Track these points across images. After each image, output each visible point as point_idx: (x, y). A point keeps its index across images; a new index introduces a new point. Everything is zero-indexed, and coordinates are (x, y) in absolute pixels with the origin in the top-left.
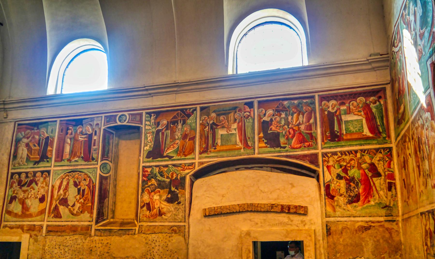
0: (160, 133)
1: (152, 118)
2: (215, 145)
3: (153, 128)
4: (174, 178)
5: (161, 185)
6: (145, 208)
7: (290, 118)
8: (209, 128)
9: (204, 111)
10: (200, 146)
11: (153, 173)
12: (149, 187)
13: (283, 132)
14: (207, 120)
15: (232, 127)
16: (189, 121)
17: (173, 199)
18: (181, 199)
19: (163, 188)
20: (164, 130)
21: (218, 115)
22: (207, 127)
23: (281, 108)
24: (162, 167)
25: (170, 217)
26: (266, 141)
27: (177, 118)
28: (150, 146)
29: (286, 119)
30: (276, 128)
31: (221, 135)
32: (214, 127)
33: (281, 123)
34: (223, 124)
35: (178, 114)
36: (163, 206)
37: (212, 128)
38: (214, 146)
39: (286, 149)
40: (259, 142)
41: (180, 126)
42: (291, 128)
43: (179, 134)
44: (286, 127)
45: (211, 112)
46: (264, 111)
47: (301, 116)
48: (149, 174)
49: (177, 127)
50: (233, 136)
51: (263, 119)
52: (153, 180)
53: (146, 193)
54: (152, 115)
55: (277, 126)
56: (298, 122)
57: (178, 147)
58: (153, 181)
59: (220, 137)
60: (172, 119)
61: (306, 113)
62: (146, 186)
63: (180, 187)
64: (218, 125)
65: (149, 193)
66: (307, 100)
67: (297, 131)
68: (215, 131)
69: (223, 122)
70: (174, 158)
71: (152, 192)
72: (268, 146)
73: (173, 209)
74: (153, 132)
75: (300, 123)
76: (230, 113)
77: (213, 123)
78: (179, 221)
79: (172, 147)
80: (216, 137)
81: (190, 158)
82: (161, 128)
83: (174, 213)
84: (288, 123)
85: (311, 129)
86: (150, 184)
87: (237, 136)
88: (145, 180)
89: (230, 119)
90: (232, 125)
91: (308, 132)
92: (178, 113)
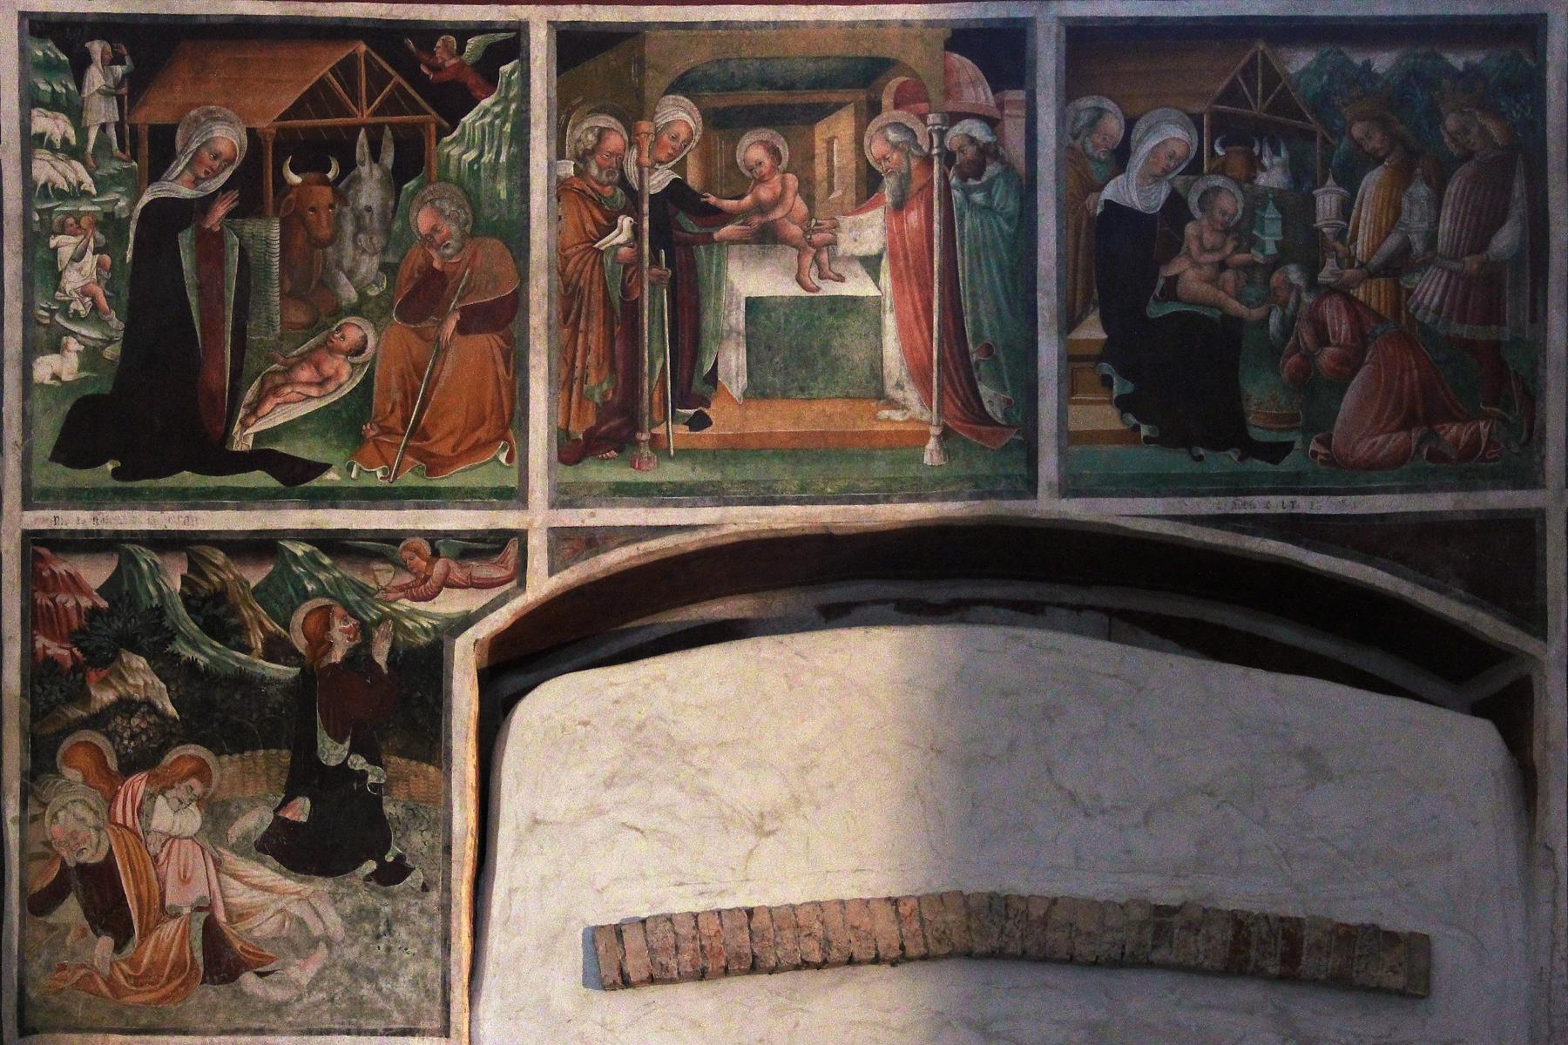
0: (185, 239)
1: (96, 78)
2: (698, 386)
4: (337, 656)
5: (219, 715)
6: (71, 911)
7: (1327, 201)
8: (636, 230)
9: (596, 67)
10: (568, 384)
11: (132, 598)
12: (98, 721)
13: (1265, 322)
14: (620, 157)
15: (847, 245)
16: (457, 152)
17: (339, 836)
20: (220, 210)
21: (725, 123)
22: (625, 222)
23: (1258, 109)
24: (219, 558)
25: (314, 984)
26: (1129, 387)
27: (343, 111)
28: (90, 357)
29: (1297, 207)
30: (1212, 281)
31: (753, 304)
32: (684, 226)
33: (1253, 242)
34: (761, 208)
35: (346, 70)
36: (240, 895)
37: (663, 234)
38: (684, 396)
39: (1288, 464)
40: (1071, 387)
41: (370, 192)
42: (1331, 290)
43: (368, 266)
44: (1294, 274)
45: (655, 82)
46: (1114, 125)
47: (1420, 190)
48: (95, 611)
49: (341, 197)
50: (855, 325)
51: (1108, 193)
52: (140, 662)
53: (73, 775)
54: (97, 48)
55: (1223, 265)
56: (1392, 242)
57: (368, 381)
58: (140, 676)
59: (738, 318)
60: (296, 110)
61: (1466, 169)
64: (725, 217)
65: (108, 782)
66: (1477, 57)
67: (1380, 319)
68: (692, 266)
69: (765, 193)
71: (129, 767)
72: (1144, 431)
73: (334, 922)
74: (110, 224)
75: (1405, 248)
76: (823, 111)
77: (677, 190)
78: (399, 1021)
79: (305, 374)
80: (708, 321)
82: (185, 192)
83: (351, 953)
84: (1306, 246)
85: (1492, 314)
86: (105, 696)
87: (890, 321)
88: (52, 663)
89: (820, 170)
90: (846, 222)
91: (1464, 331)
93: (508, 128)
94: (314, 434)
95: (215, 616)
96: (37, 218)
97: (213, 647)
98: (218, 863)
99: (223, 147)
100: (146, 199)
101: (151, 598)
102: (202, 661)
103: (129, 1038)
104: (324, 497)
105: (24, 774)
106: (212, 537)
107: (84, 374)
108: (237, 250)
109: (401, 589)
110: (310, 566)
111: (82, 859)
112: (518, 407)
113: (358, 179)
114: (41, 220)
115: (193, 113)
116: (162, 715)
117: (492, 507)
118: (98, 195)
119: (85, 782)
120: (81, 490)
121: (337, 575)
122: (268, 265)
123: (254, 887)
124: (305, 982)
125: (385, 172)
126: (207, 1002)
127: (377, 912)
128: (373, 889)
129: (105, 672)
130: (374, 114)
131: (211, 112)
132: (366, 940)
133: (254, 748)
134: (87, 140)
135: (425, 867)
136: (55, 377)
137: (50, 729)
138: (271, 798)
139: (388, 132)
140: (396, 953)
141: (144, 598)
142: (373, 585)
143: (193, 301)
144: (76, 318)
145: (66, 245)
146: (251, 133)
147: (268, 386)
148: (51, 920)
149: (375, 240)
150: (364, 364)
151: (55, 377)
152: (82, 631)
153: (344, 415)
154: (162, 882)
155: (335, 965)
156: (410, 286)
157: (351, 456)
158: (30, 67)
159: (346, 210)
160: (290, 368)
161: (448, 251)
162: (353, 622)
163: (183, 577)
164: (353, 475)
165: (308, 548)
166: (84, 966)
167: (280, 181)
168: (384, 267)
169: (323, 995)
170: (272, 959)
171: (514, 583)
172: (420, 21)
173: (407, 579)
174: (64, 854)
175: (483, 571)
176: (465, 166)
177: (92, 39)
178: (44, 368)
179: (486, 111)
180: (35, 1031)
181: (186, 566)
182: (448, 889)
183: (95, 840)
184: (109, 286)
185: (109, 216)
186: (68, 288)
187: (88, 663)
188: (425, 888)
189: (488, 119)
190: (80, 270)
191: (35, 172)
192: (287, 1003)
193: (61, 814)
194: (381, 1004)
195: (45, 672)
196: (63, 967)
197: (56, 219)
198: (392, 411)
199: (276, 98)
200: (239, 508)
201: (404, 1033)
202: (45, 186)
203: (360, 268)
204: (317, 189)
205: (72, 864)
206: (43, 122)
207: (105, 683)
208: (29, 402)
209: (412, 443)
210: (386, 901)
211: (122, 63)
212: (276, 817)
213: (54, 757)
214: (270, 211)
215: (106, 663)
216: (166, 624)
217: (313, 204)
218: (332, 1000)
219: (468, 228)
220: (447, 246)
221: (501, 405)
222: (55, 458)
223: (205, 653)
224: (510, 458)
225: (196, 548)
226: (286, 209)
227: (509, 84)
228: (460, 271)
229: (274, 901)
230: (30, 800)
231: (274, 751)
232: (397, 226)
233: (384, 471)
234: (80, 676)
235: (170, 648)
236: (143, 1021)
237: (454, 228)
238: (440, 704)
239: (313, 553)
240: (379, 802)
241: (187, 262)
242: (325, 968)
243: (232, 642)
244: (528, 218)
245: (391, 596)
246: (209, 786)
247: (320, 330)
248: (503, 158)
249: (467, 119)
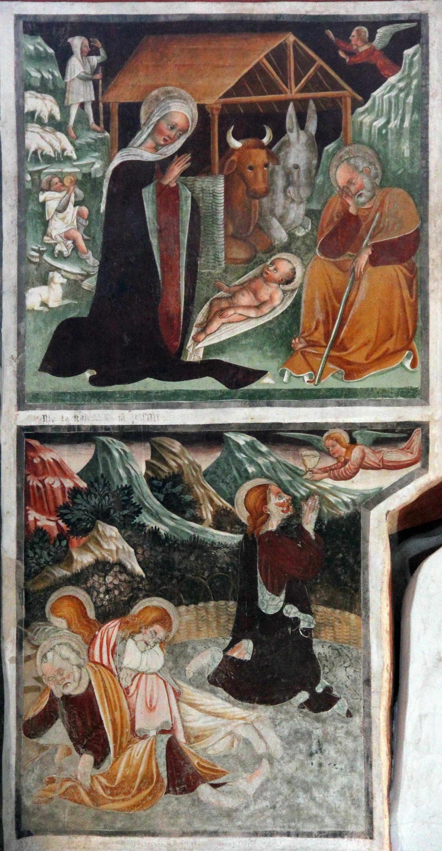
0: (148, 194)
1: (76, 66)
3: (91, 147)
4: (273, 525)
5: (176, 574)
6: (58, 734)
11: (106, 481)
12: (78, 579)
16: (367, 119)
18: (337, 677)
20: (176, 170)
24: (177, 446)
25: (260, 793)
28: (72, 288)
35: (278, 57)
36: (197, 721)
41: (297, 151)
43: (296, 212)
48: (76, 491)
49: (274, 158)
52: (112, 531)
53: (60, 623)
54: (77, 43)
57: (296, 304)
58: (112, 542)
60: (238, 89)
62: (60, 572)
63: (322, 594)
65: (88, 628)
70: (267, 382)
71: (104, 616)
73: (274, 743)
74: (88, 183)
78: (330, 826)
79: (245, 299)
81: (384, 393)
82: (148, 156)
83: (290, 768)
86: (83, 559)
88: (42, 532)
92: (282, 48)
93: (410, 99)
94: (253, 348)
95: (174, 494)
96: (28, 178)
97: (173, 519)
98: (178, 694)
99: (178, 120)
100: (116, 162)
101: (121, 479)
102: (163, 530)
103: (107, 839)
104: (261, 398)
105: (19, 623)
106: (171, 430)
107: (67, 302)
108: (189, 202)
109: (325, 470)
110: (250, 452)
111: (67, 691)
112: (420, 324)
113: (288, 144)
114: (33, 180)
115: (155, 93)
116: (132, 574)
117: (399, 404)
118: (78, 159)
119: (69, 628)
120: (64, 394)
121: (272, 459)
122: (214, 214)
123: (209, 713)
124: (251, 791)
125: (309, 137)
126: (170, 808)
127: (310, 734)
128: (306, 715)
129: (84, 539)
130: (301, 91)
131: (169, 92)
132: (301, 757)
133: (207, 600)
134: (68, 116)
135: (349, 696)
136: (44, 304)
137: (41, 586)
138: (221, 641)
139: (311, 103)
140: (326, 767)
141: (116, 479)
142: (302, 468)
143: (154, 241)
144: (61, 256)
145: (52, 200)
146: (201, 108)
147: (215, 309)
148: (42, 741)
149: (301, 191)
150: (293, 291)
151: (44, 304)
152: (66, 506)
153: (277, 331)
154: (132, 710)
155: (275, 778)
156: (331, 228)
157: (285, 364)
158: (23, 59)
159: (277, 168)
160: (233, 295)
161: (362, 199)
162: (286, 497)
163: (147, 463)
164: (285, 379)
165: (249, 438)
166: (68, 780)
167: (224, 146)
168: (309, 213)
169: (266, 803)
170: (224, 773)
171: (418, 465)
172: (338, 16)
173: (330, 462)
174: (53, 687)
175: (392, 455)
176: (375, 131)
177: (73, 34)
178: (35, 297)
179: (393, 87)
180: (29, 834)
181: (149, 452)
182: (368, 715)
183: (77, 675)
184: (87, 231)
185: (87, 176)
186: (54, 234)
187: (71, 532)
188: (349, 714)
189: (393, 93)
190: (63, 219)
191: (27, 142)
192: (237, 810)
193: (50, 655)
194: (314, 811)
195: (36, 540)
196: (52, 781)
197: (45, 179)
198: (316, 329)
199: (220, 81)
200: (192, 407)
201: (335, 835)
202: (35, 153)
203: (289, 214)
204: (254, 151)
205: (58, 695)
206: (33, 102)
207: (85, 548)
208: (23, 324)
209: (334, 353)
210: (317, 725)
211: (98, 54)
212: (226, 657)
213: (44, 608)
214: (217, 169)
215: (86, 531)
216: (134, 500)
217: (251, 164)
218: (274, 807)
219: (378, 181)
220: (360, 195)
221: (407, 322)
222: (43, 368)
223: (166, 523)
224: (413, 365)
225: (158, 439)
226: (230, 169)
227: (411, 64)
228: (371, 215)
229: (224, 725)
230: (24, 643)
231: (222, 603)
232: (319, 180)
233: (310, 376)
234: (64, 543)
235: (137, 520)
236: (119, 825)
237: (366, 181)
238: (358, 563)
239: (253, 442)
240: (309, 644)
241: (150, 211)
242: (268, 780)
243: (188, 515)
244: (427, 172)
245: (317, 476)
246: (170, 631)
247: (257, 264)
248: (406, 124)
249: (377, 94)
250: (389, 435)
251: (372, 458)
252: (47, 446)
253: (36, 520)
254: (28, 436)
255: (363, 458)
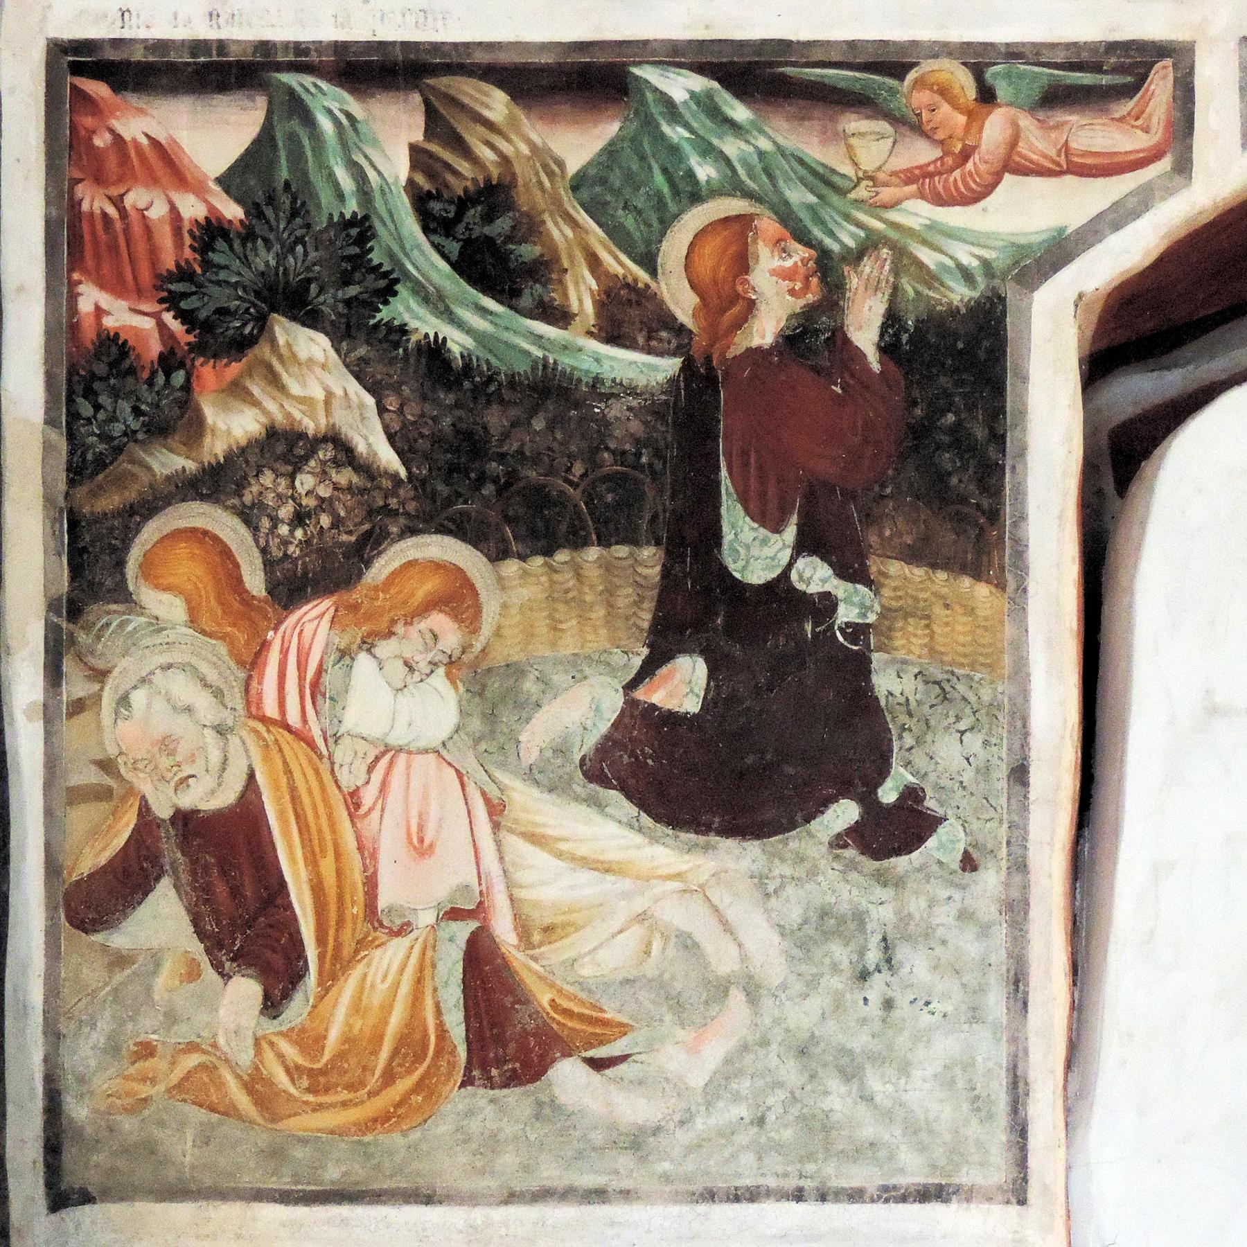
4: (764, 331)
5: (492, 467)
6: (162, 920)
18: (935, 761)
19: (528, 520)
25: (717, 1088)
36: (547, 883)
48: (212, 232)
52: (312, 345)
58: (313, 377)
62: (168, 462)
63: (897, 526)
65: (244, 619)
71: (290, 589)
73: (762, 943)
78: (914, 1173)
83: (803, 1015)
86: (231, 425)
88: (115, 349)
95: (489, 240)
97: (483, 311)
98: (496, 810)
101: (341, 197)
102: (458, 343)
103: (301, 1212)
105: (53, 606)
106: (481, 57)
109: (909, 176)
110: (701, 123)
111: (187, 801)
116: (366, 469)
119: (193, 621)
121: (765, 144)
124: (697, 1080)
126: (474, 1126)
127: (860, 918)
128: (852, 866)
129: (235, 368)
132: (836, 983)
133: (577, 541)
138: (618, 658)
141: (326, 197)
142: (847, 169)
148: (119, 939)
152: (184, 274)
154: (368, 852)
155: (764, 1043)
162: (800, 253)
163: (414, 149)
165: (699, 83)
166: (192, 1047)
169: (742, 1110)
170: (623, 1029)
174: (146, 787)
180: (86, 1198)
183: (215, 756)
187: (199, 348)
188: (969, 864)
192: (657, 1131)
193: (139, 698)
194: (869, 1131)
196: (147, 1050)
205: (163, 812)
207: (237, 391)
210: (880, 893)
212: (631, 703)
213: (121, 564)
215: (241, 345)
216: (376, 257)
218: (761, 1121)
223: (465, 323)
225: (444, 82)
229: (625, 896)
230: (68, 665)
231: (622, 551)
234: (179, 378)
235: (384, 314)
236: (332, 1174)
238: (999, 439)
239: (709, 95)
240: (861, 666)
242: (745, 1048)
243: (526, 301)
245: (887, 194)
246: (475, 631)
250: (1086, 78)
251: (1038, 142)
252: (133, 99)
253: (99, 312)
254: (78, 69)
255: (1013, 144)
